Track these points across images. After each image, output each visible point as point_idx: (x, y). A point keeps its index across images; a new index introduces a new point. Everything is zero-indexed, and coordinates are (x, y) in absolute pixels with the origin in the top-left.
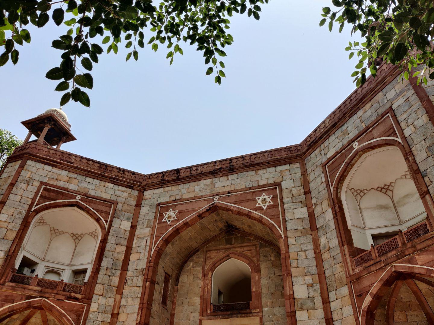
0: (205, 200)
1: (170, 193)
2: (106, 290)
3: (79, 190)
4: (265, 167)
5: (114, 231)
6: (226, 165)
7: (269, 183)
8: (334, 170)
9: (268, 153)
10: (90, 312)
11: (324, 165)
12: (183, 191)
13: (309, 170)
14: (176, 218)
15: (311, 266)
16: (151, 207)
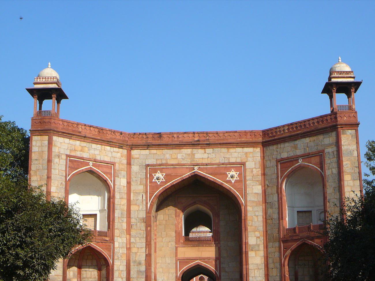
2: (121, 233)
3: (91, 157)
4: (235, 147)
5: (118, 189)
6: (204, 139)
11: (278, 161)
12: (168, 156)
13: (266, 158)
14: (164, 180)
15: (260, 225)
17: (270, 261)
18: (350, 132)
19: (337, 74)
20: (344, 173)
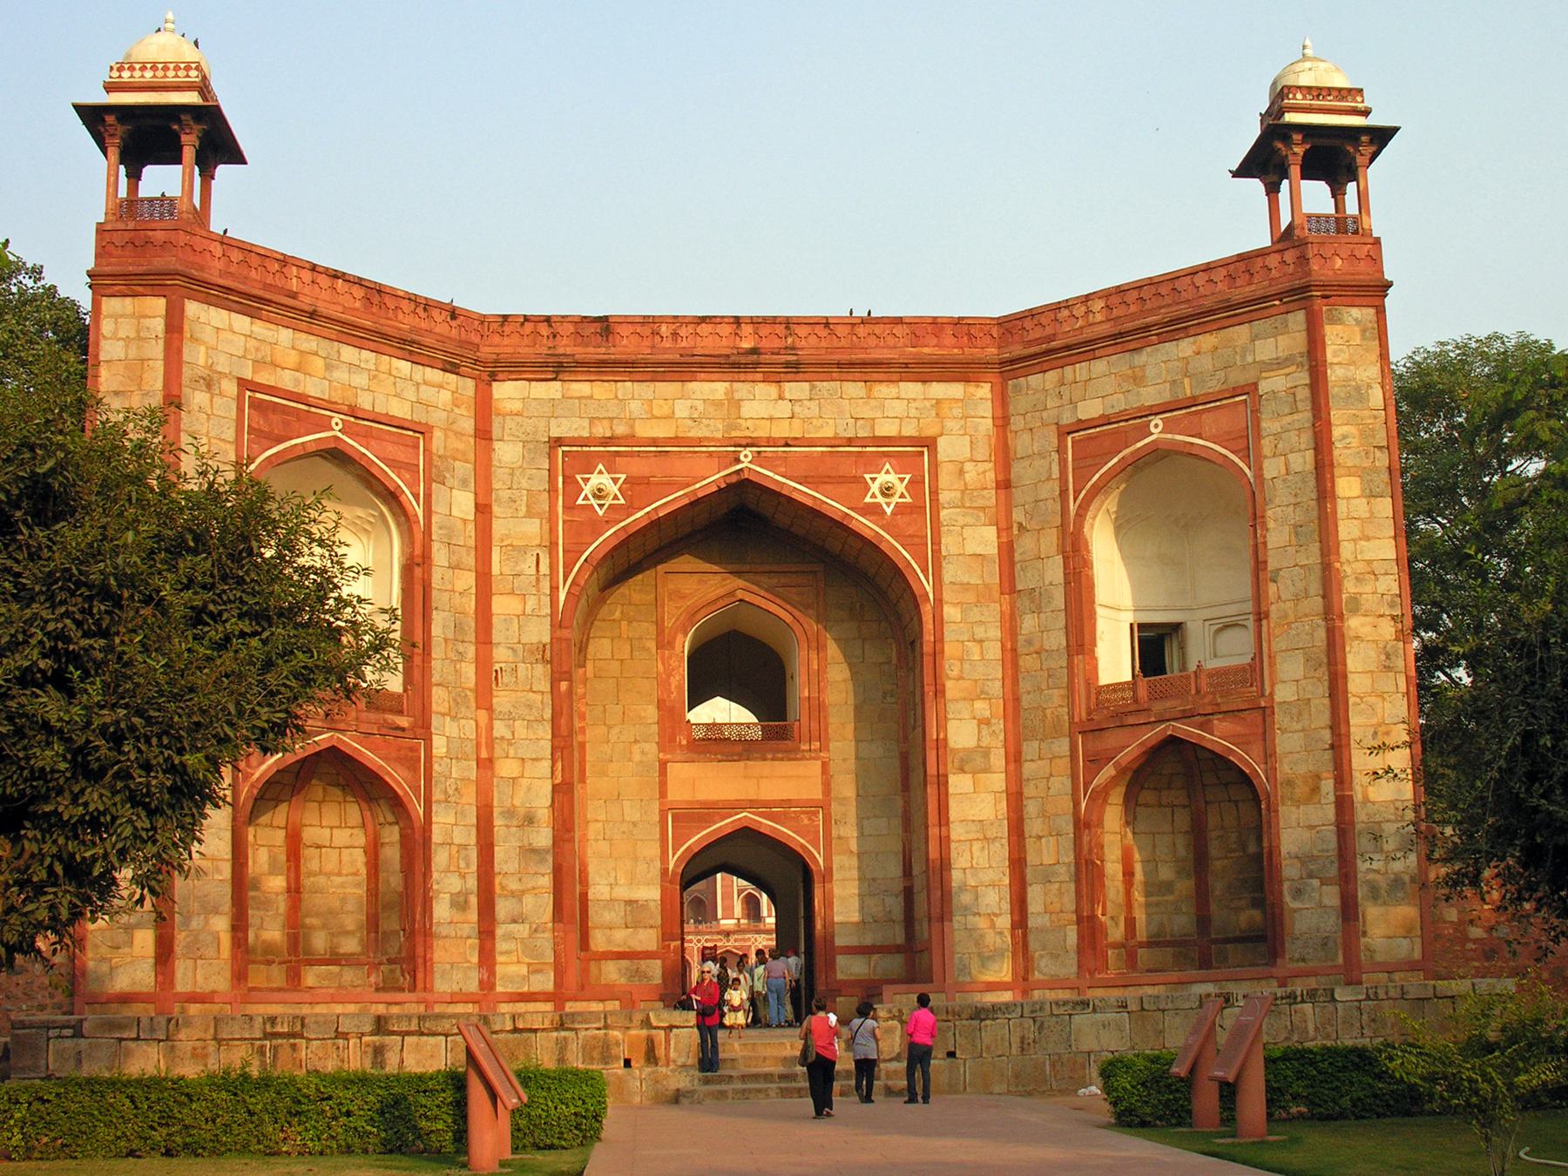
0: (711, 454)
6: (777, 343)
7: (904, 433)
8: (1089, 462)
11: (1064, 432)
12: (635, 407)
13: (1017, 423)
14: (622, 501)
17: (1031, 808)
18: (1359, 314)
19: (1304, 98)
20: (1337, 471)
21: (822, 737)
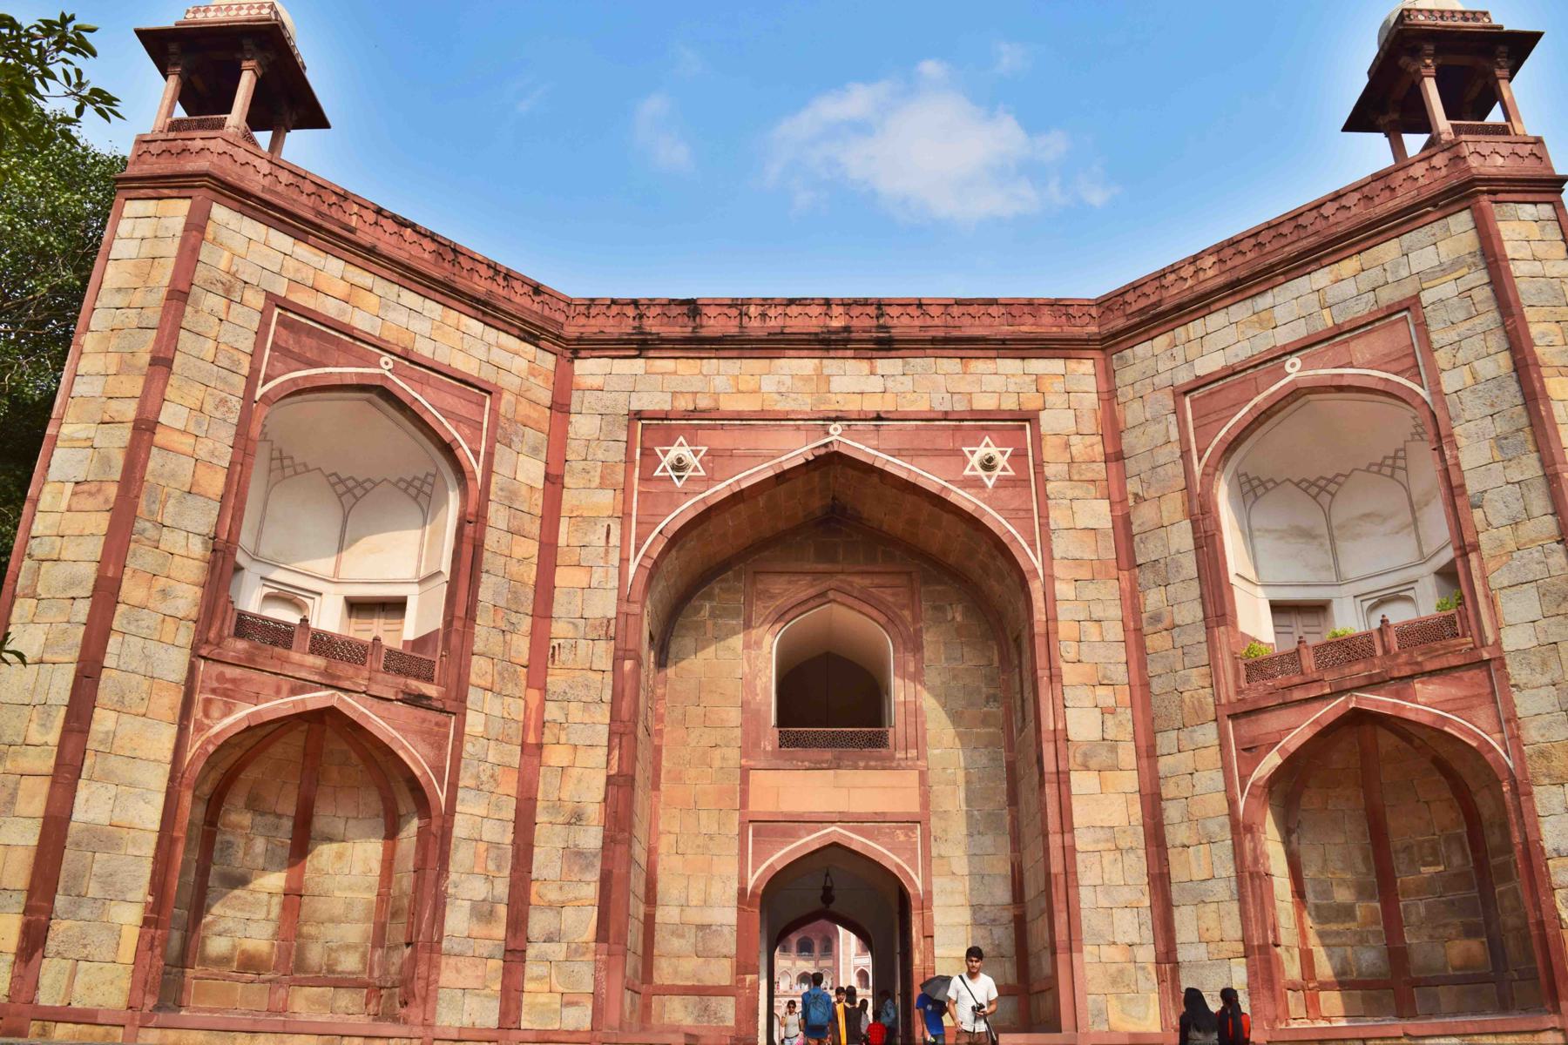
1: (674, 384)
2: (500, 674)
4: (992, 353)
6: (868, 322)
7: (1004, 407)
8: (1214, 417)
9: (1003, 310)
10: (466, 738)
12: (720, 383)
13: (1125, 393)
14: (702, 473)
16: (610, 418)
17: (1172, 812)
21: (918, 742)
